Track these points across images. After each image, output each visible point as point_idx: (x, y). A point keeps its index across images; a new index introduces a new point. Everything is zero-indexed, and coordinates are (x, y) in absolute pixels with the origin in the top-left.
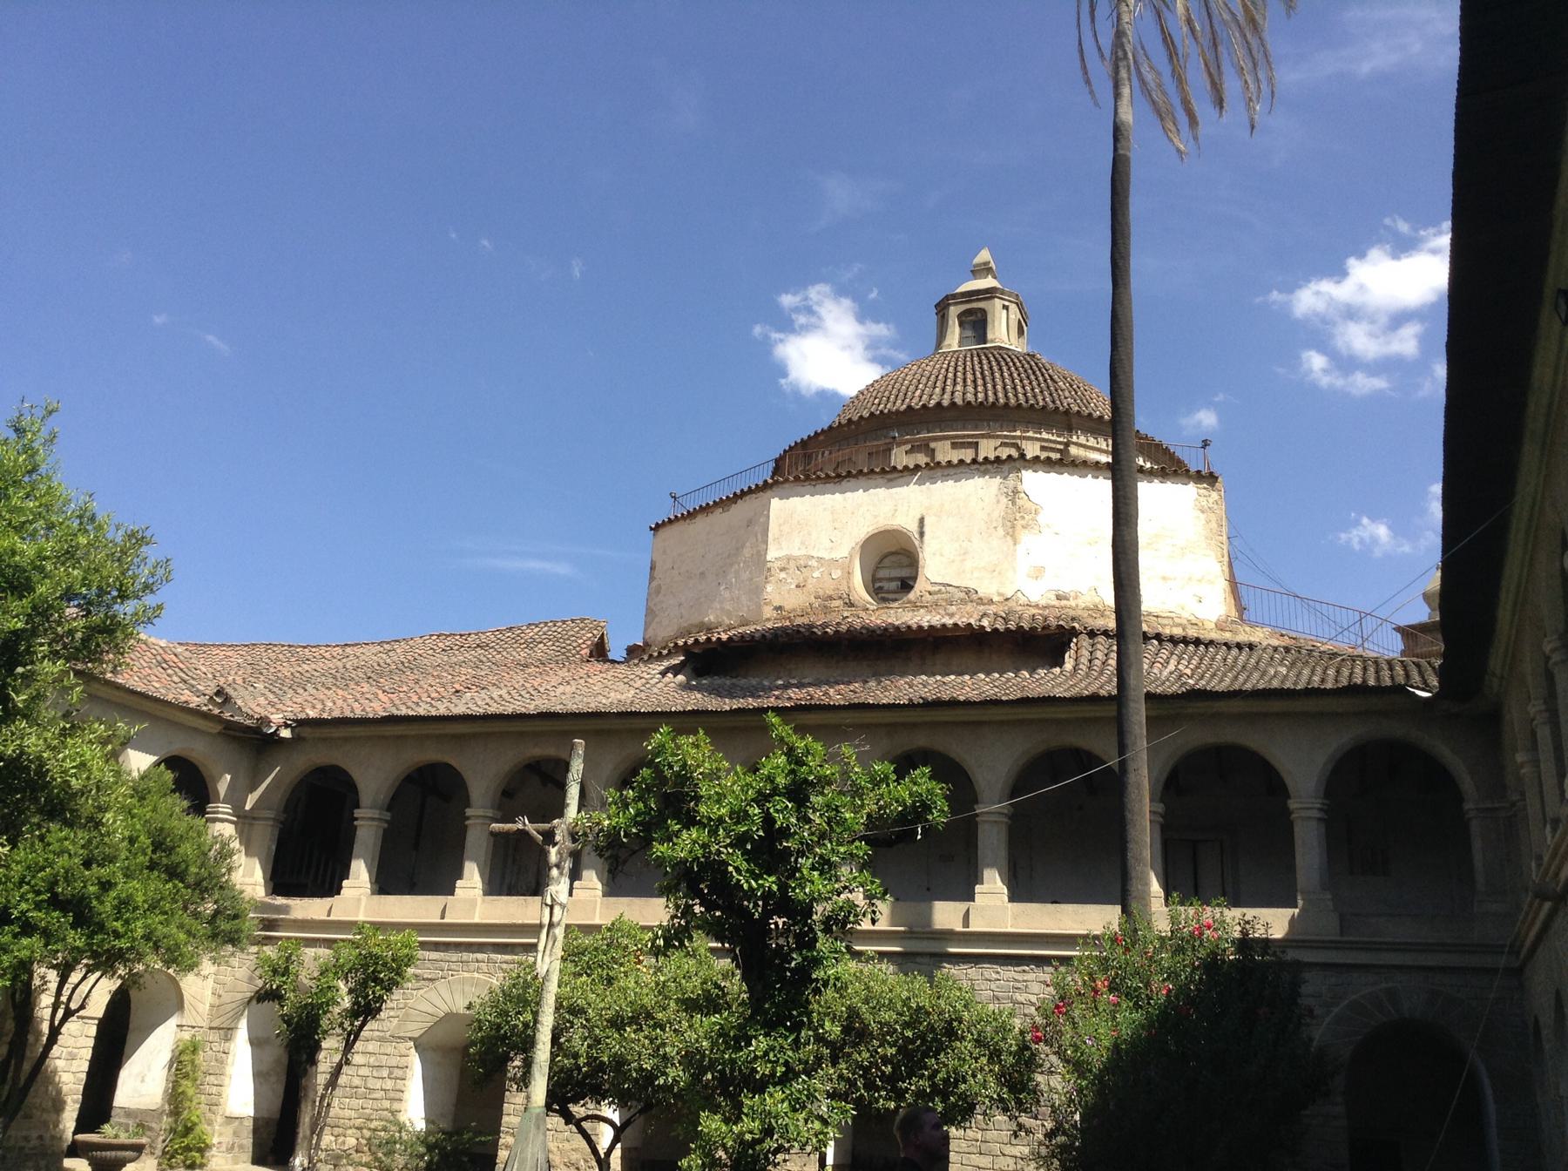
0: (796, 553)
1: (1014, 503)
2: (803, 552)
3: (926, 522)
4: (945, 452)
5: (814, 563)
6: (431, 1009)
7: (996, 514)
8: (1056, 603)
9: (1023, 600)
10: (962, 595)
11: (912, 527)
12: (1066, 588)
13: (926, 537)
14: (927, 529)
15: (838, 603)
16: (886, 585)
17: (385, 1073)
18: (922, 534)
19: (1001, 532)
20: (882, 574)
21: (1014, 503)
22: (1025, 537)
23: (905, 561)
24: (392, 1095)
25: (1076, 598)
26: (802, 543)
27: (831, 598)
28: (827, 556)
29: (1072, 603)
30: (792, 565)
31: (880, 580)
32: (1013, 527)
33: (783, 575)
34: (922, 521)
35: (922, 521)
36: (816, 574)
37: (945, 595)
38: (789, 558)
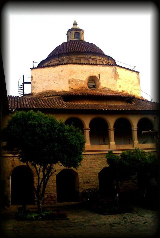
0: (74, 78)
1: (115, 73)
2: (76, 78)
3: (100, 75)
4: (82, 61)
5: (79, 81)
6: (59, 169)
7: (113, 75)
8: (122, 92)
9: (118, 91)
10: (108, 89)
11: (98, 76)
12: (123, 90)
13: (101, 78)
14: (100, 76)
15: (84, 89)
16: (90, 86)
17: (51, 182)
18: (99, 77)
19: (114, 79)
20: (89, 84)
21: (115, 73)
22: (118, 80)
23: (93, 82)
24: (53, 186)
25: (125, 91)
26: (76, 76)
27: (83, 88)
28: (81, 79)
29: (124, 92)
30: (74, 80)
31: (89, 85)
32: (116, 78)
33: (72, 82)
34: (99, 75)
35: (99, 75)
36: (79, 83)
37: (104, 90)
38: (73, 79)
